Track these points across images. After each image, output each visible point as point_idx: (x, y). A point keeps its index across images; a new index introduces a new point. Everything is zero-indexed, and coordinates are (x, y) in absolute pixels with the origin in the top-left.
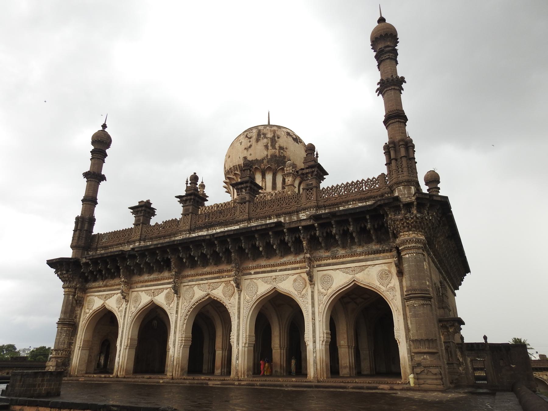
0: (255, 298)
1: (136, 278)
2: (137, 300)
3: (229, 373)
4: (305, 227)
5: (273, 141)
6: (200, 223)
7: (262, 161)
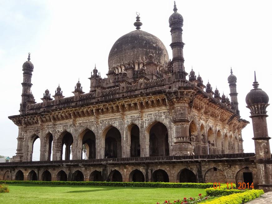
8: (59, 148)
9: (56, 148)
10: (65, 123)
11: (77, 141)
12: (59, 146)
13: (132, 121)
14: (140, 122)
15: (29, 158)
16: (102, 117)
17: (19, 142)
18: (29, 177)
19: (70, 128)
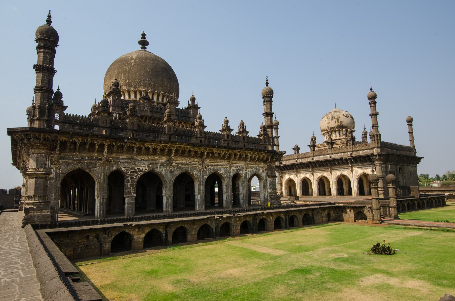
0: (336, 176)
1: (298, 170)
2: (300, 176)
3: (331, 195)
4: (349, 159)
5: (338, 119)
6: (317, 154)
7: (334, 128)
10: (152, 160)
13: (237, 170)
14: (244, 172)
16: (208, 162)
19: (160, 168)
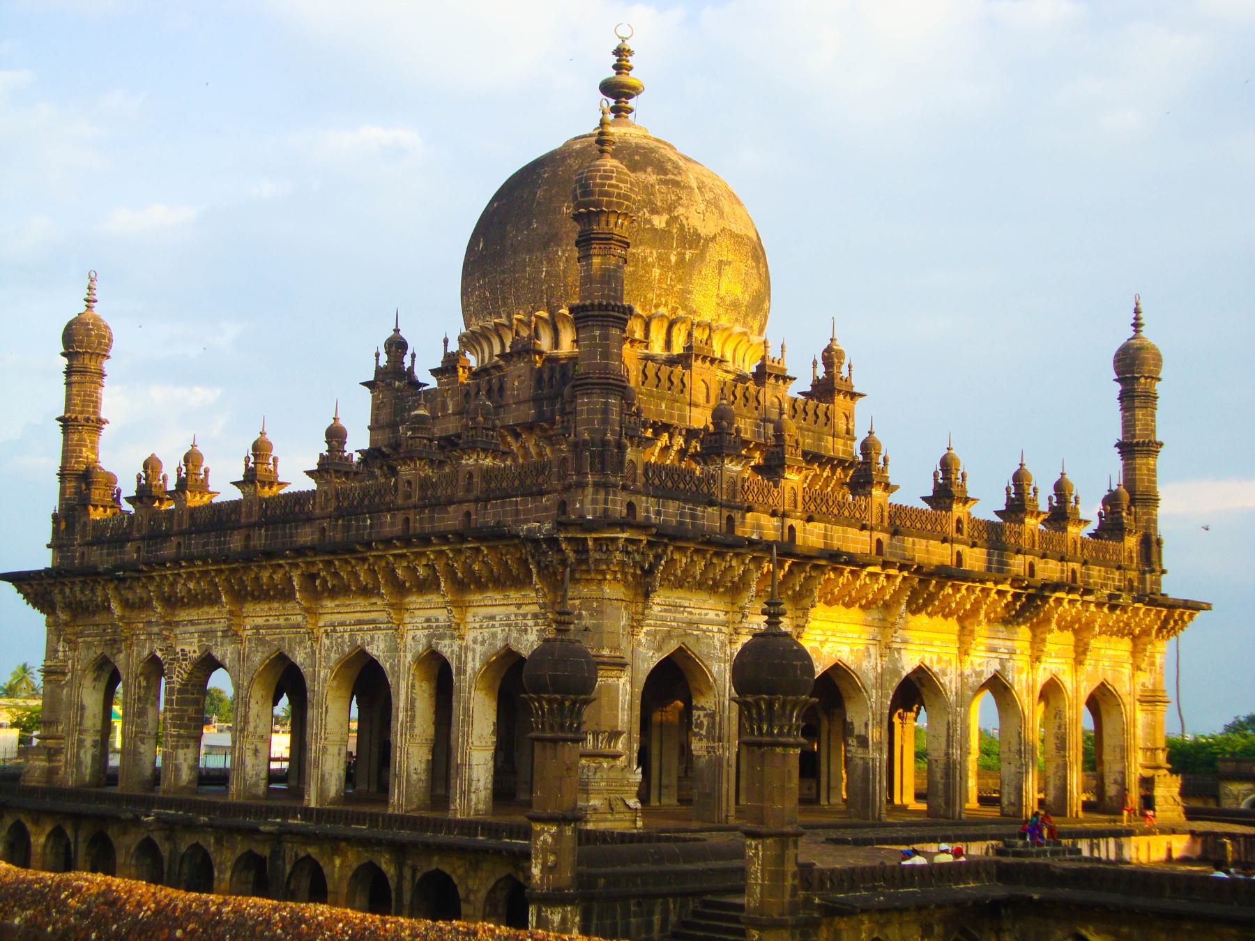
8: (187, 727)
9: (174, 726)
11: (247, 705)
12: (190, 719)
15: (87, 756)
17: (49, 687)
18: (48, 851)
